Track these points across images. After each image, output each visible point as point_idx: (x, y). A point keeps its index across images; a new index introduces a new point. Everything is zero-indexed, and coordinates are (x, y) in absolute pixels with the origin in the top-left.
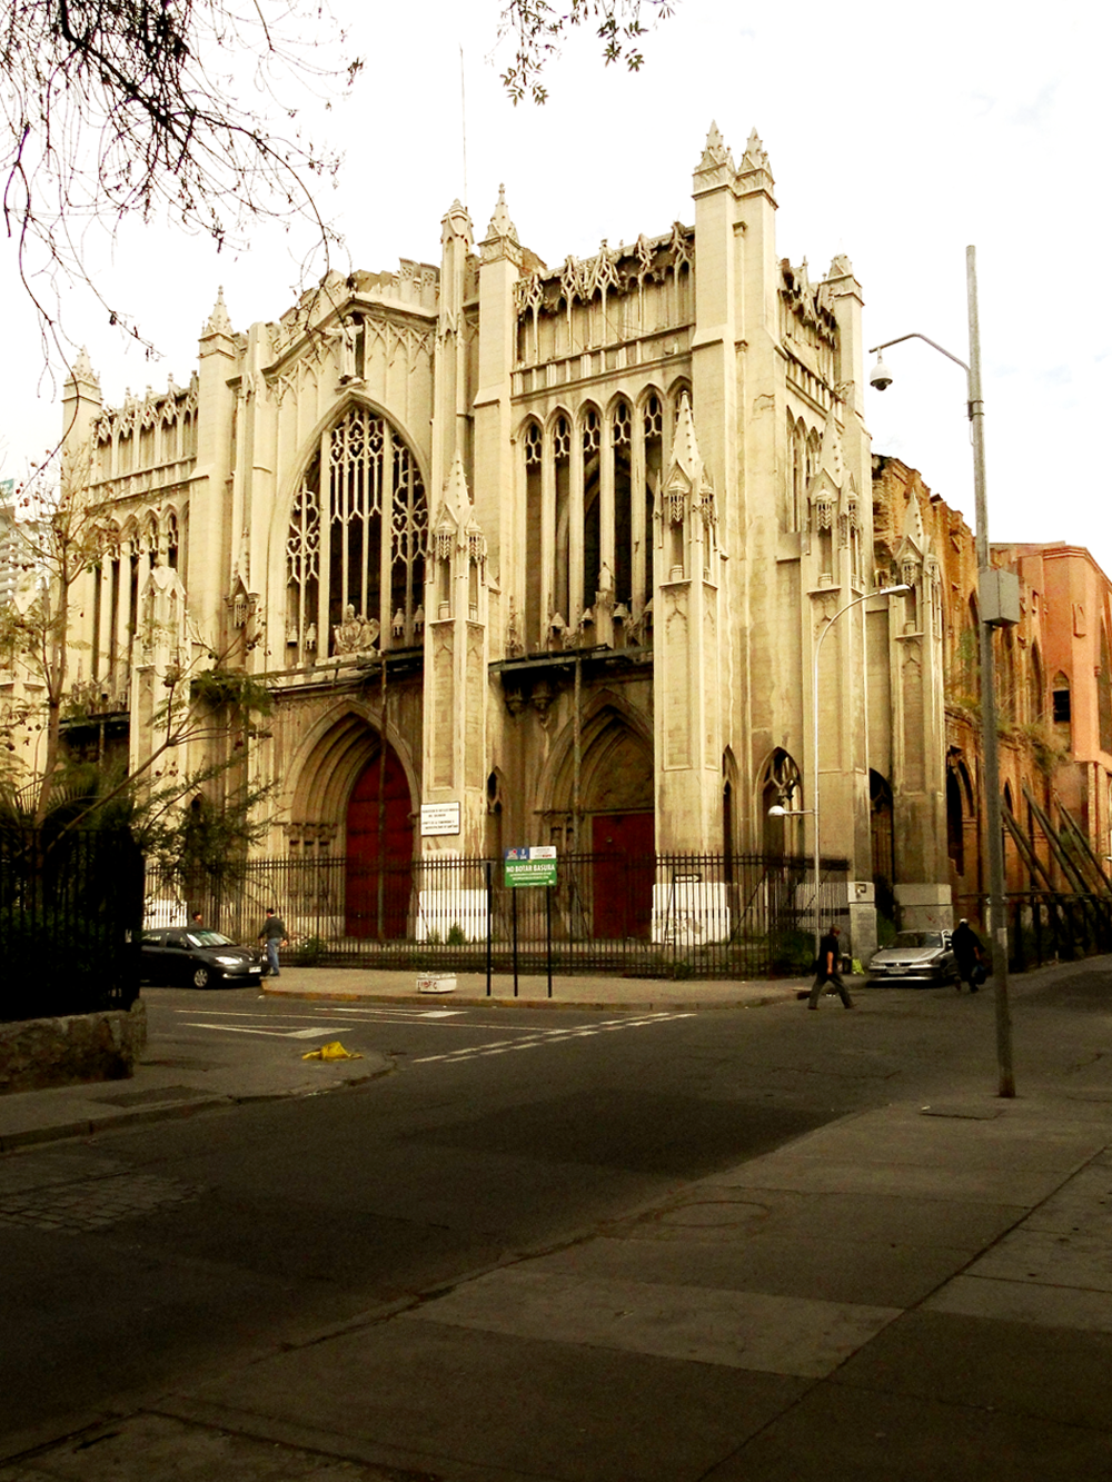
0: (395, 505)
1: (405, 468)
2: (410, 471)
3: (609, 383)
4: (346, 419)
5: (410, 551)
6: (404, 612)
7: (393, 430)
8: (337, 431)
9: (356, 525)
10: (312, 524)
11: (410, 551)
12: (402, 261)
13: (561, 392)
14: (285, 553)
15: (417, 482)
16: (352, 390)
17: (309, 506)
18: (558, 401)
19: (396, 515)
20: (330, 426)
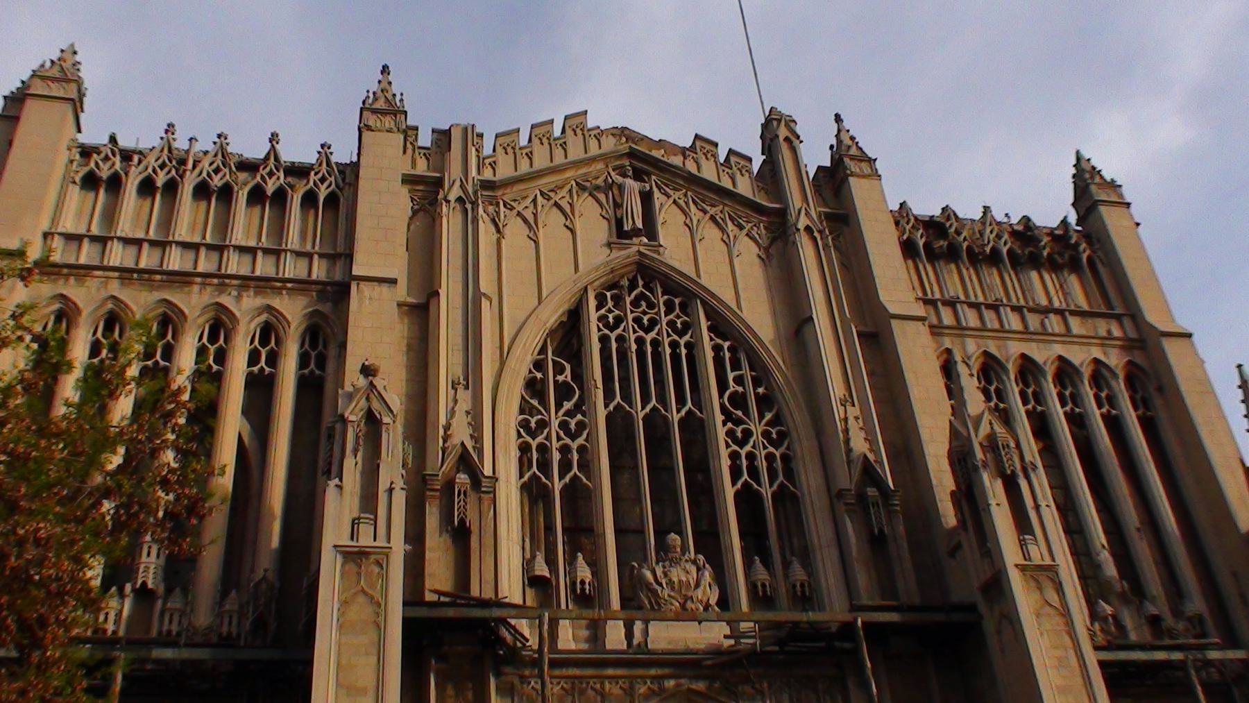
0: (724, 410)
1: (736, 365)
2: (746, 371)
3: (1041, 345)
4: (625, 282)
5: (765, 477)
6: (767, 564)
7: (711, 314)
8: (608, 294)
9: (656, 424)
10: (568, 405)
11: (765, 477)
12: (697, 137)
13: (982, 337)
14: (514, 434)
15: (761, 390)
16: (642, 249)
17: (560, 378)
18: (979, 346)
19: (730, 425)
20: (597, 283)
